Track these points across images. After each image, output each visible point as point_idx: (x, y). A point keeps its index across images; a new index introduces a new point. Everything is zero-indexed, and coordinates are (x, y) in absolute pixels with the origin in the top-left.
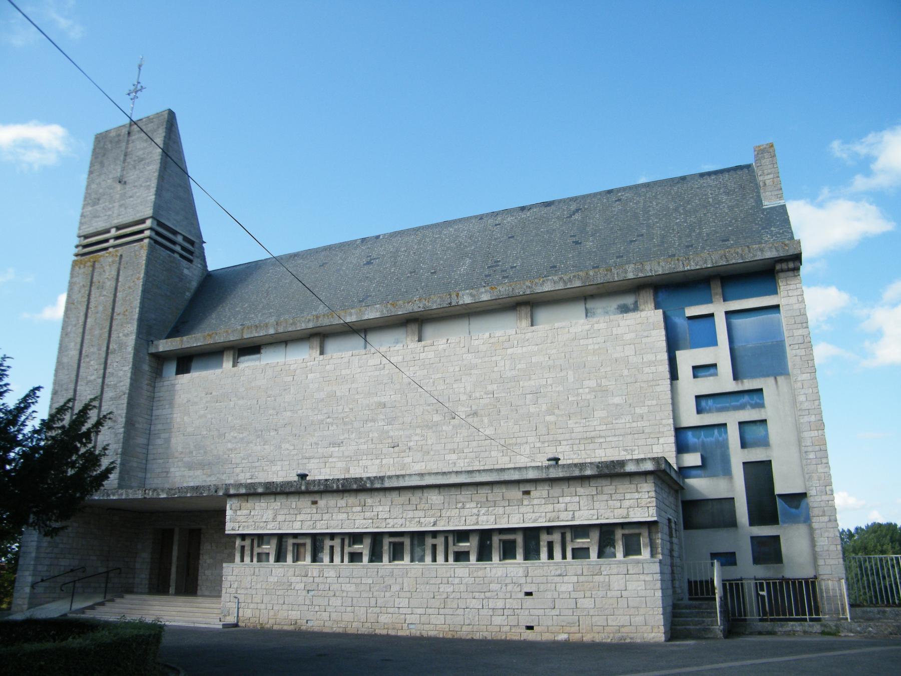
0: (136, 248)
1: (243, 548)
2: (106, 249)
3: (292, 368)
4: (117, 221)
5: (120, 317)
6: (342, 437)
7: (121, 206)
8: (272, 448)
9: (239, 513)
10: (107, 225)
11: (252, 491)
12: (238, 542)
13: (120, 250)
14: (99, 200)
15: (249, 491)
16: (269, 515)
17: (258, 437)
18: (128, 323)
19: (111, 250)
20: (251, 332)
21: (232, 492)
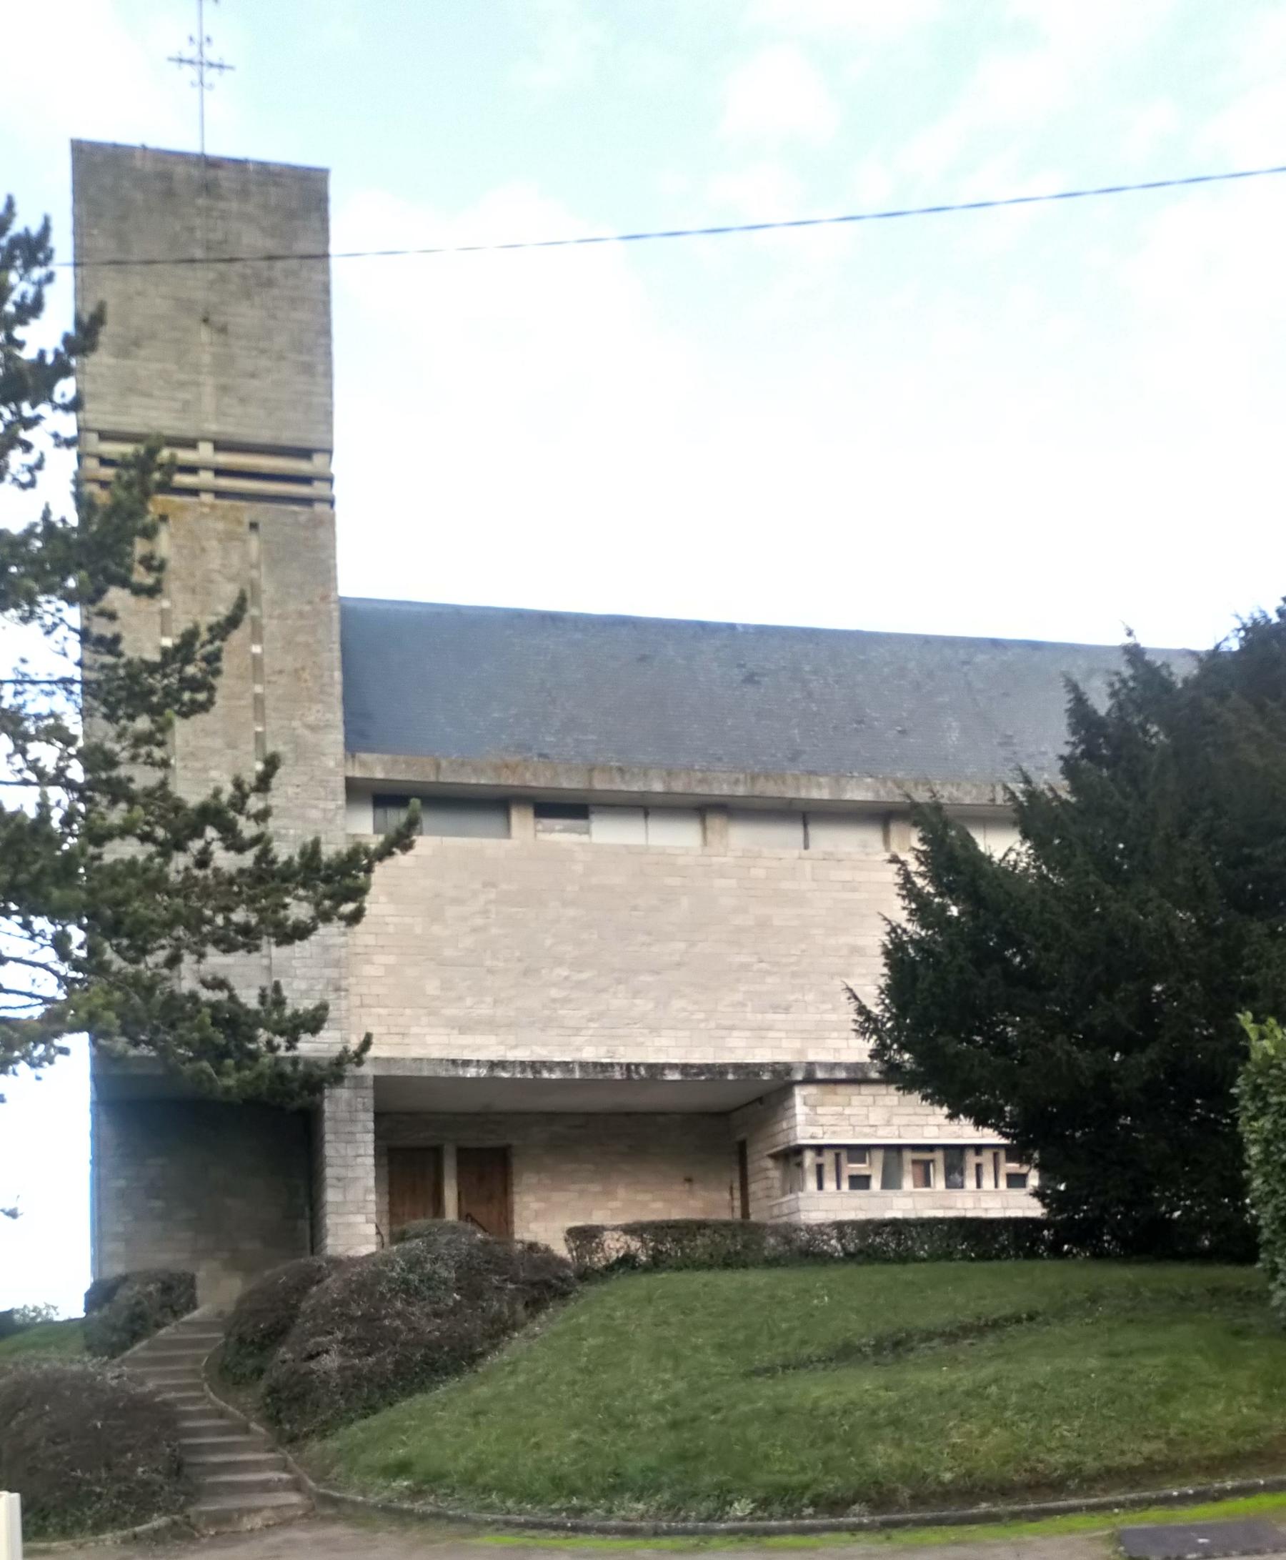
0: (302, 518)
1: (820, 1169)
2: (194, 492)
3: (681, 861)
4: (212, 427)
5: (283, 680)
6: (792, 998)
7: (224, 389)
8: (651, 1005)
9: (820, 1110)
10: (184, 428)
11: (860, 1076)
12: (809, 1159)
13: (250, 511)
14: (137, 343)
15: (852, 1076)
16: (876, 1116)
17: (619, 982)
18: (312, 700)
19: (207, 498)
20: (612, 781)
21: (820, 1075)
